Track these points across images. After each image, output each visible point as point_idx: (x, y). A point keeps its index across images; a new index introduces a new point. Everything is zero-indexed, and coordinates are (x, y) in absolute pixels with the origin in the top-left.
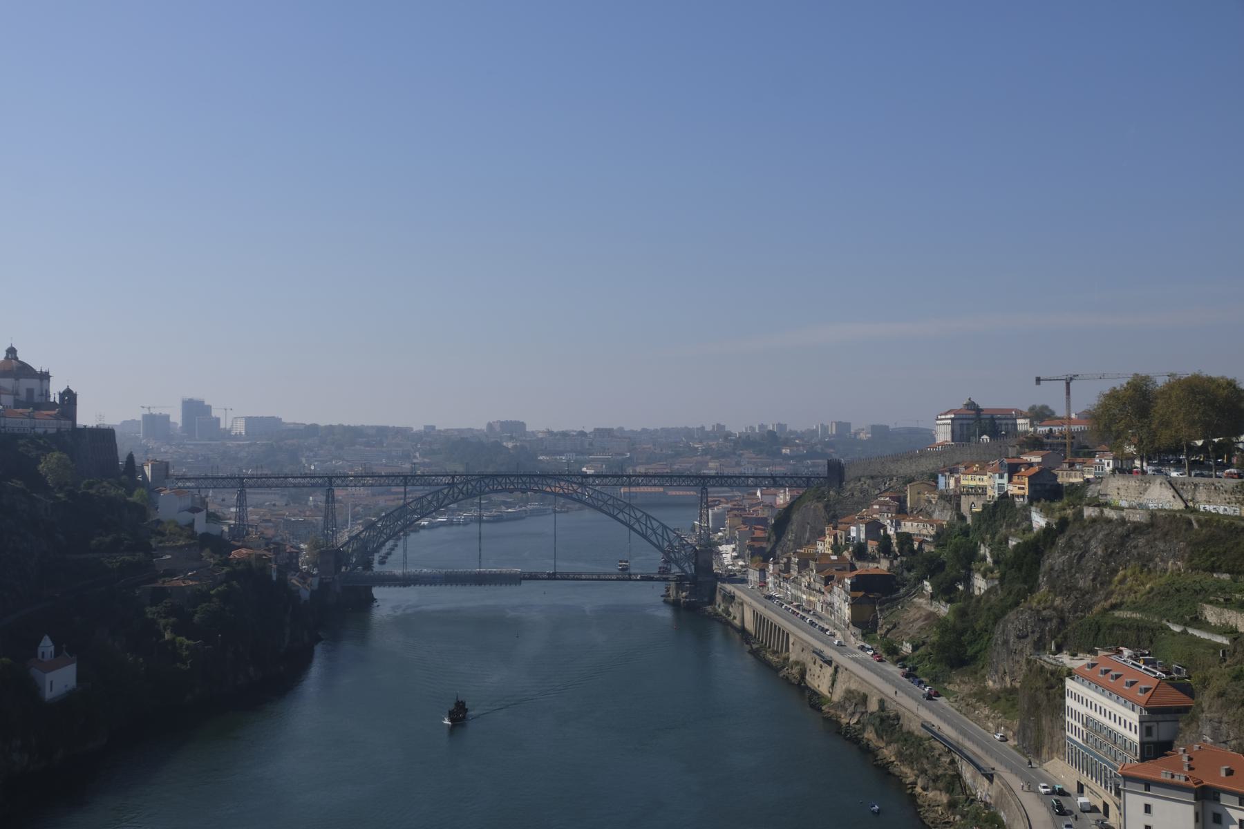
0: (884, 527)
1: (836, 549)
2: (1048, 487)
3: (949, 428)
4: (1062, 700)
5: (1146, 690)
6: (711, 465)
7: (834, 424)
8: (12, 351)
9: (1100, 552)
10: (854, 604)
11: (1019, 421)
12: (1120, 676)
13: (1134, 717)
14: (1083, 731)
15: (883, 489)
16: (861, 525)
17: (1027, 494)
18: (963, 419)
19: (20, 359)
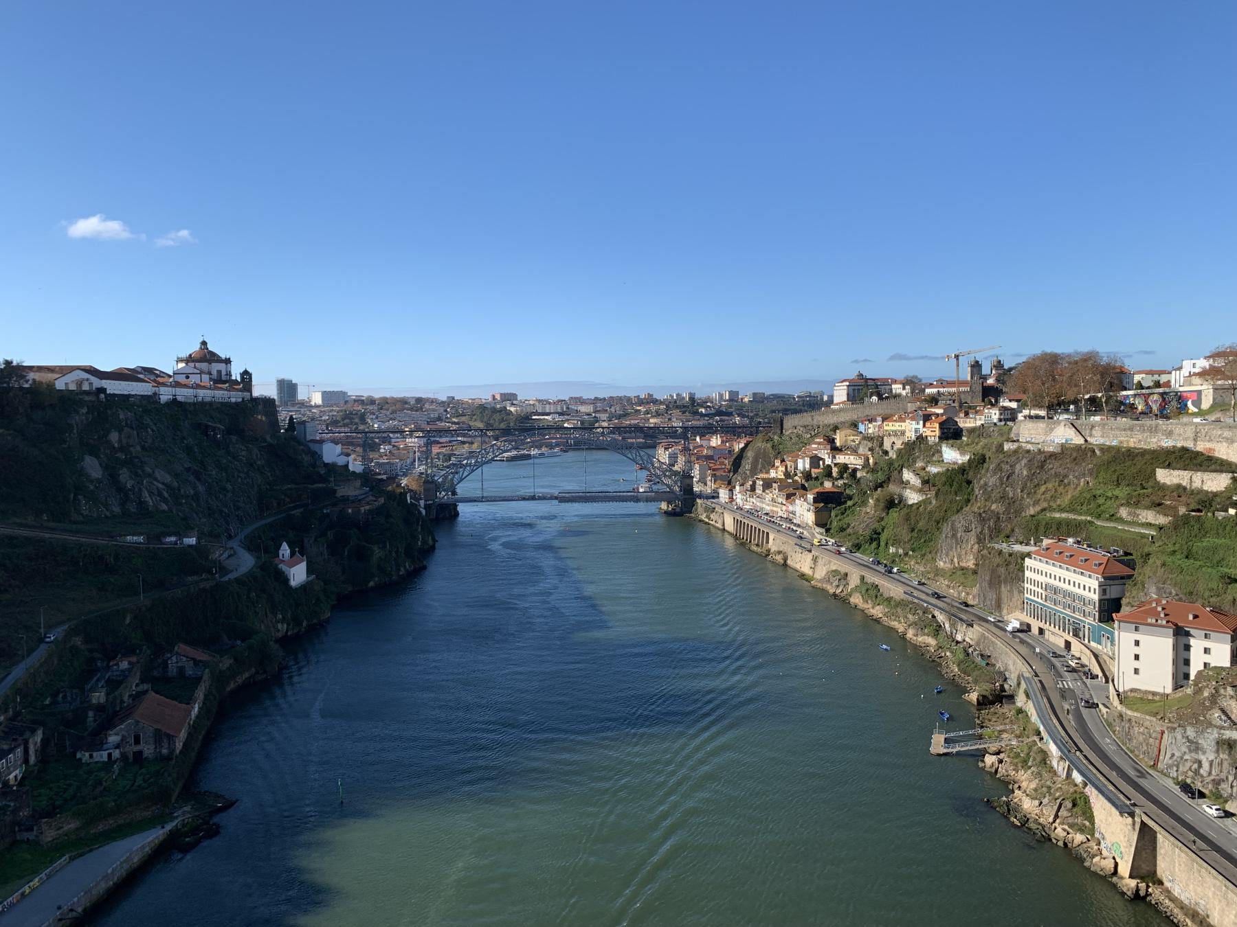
0: (823, 460)
1: (787, 475)
2: (952, 431)
3: (845, 392)
4: (1021, 574)
5: (1100, 564)
6: (651, 421)
7: (727, 392)
8: (204, 343)
9: (1025, 473)
10: (818, 512)
11: (894, 386)
12: (1073, 555)
13: (1094, 584)
14: (1042, 594)
15: (813, 434)
16: (806, 458)
17: (938, 435)
18: (854, 386)
19: (210, 349)
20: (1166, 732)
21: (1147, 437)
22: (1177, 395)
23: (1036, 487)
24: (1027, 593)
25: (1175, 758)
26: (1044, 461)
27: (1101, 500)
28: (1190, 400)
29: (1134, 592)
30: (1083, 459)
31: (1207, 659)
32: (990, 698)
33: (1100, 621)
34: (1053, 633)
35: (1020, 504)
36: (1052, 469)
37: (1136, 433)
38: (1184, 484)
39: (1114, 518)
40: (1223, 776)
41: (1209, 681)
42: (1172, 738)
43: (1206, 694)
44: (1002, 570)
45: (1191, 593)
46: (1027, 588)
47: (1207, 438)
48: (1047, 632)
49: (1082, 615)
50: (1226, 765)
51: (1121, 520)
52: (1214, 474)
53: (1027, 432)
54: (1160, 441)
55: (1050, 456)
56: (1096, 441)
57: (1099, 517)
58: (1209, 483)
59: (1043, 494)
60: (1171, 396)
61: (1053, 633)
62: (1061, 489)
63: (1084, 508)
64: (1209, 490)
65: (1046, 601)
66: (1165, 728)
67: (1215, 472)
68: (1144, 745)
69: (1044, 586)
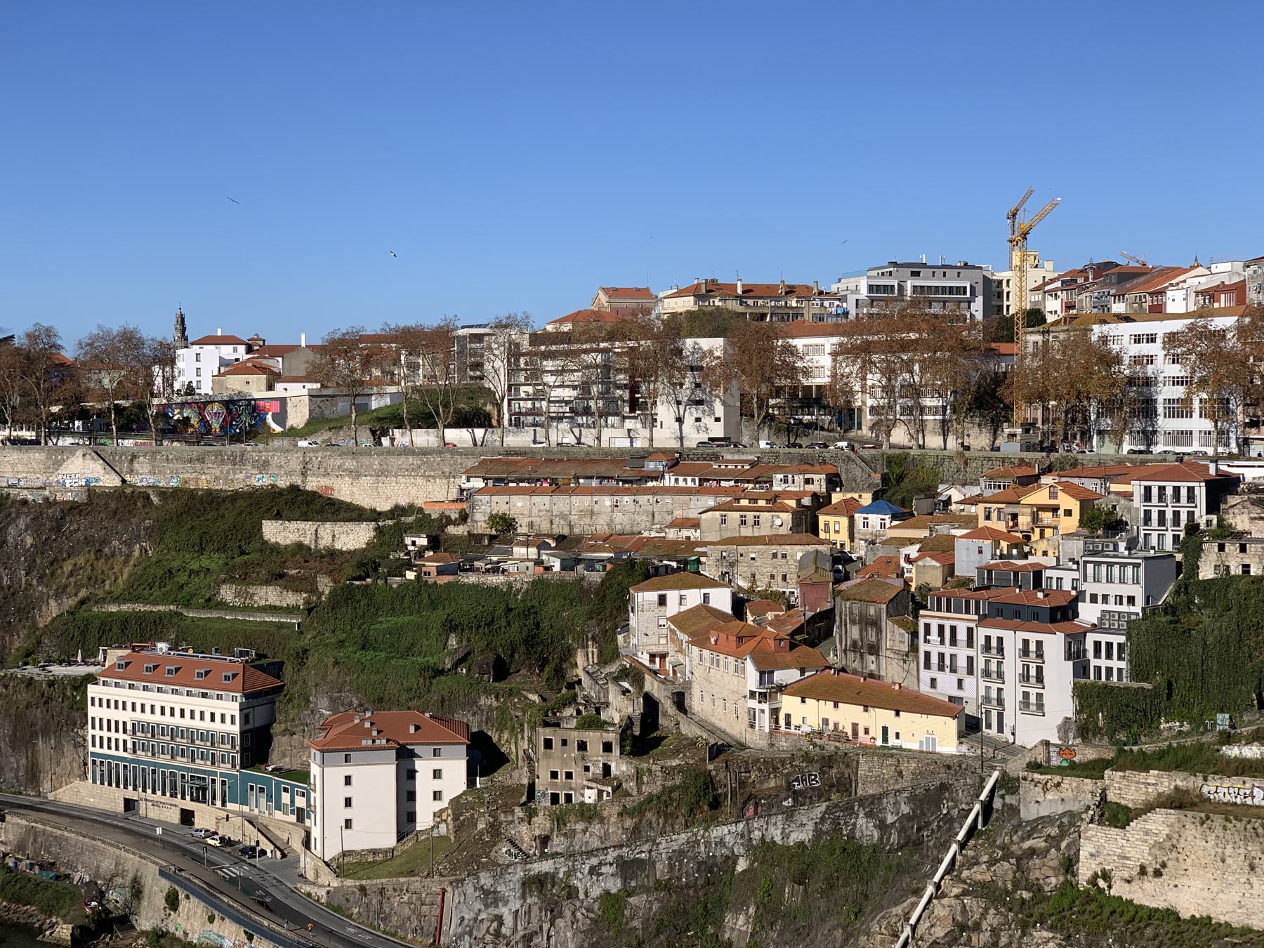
5: (234, 676)
13: (230, 706)
20: (449, 889)
21: (228, 472)
22: (249, 404)
23: (52, 563)
24: (94, 745)
25: (466, 922)
26: (61, 519)
27: (182, 578)
28: (270, 413)
29: (292, 713)
30: (130, 512)
31: (437, 785)
32: (92, 926)
33: (242, 767)
34: (155, 804)
35: (26, 597)
36: (76, 531)
37: (210, 465)
38: (307, 542)
39: (212, 603)
40: (534, 926)
41: (473, 809)
42: (459, 896)
43: (481, 826)
44: (38, 714)
45: (381, 700)
46: (93, 737)
47: (322, 470)
48: (142, 804)
49: (209, 763)
50: (535, 909)
51: (223, 605)
52: (350, 525)
53: (8, 469)
54: (250, 478)
55: (71, 509)
56: (141, 481)
57: (188, 605)
58: (343, 538)
59: (71, 574)
60: (240, 406)
61: (155, 804)
62: (100, 564)
63: (156, 592)
64: (344, 549)
65: (134, 752)
66: (445, 885)
67: (352, 520)
68: (414, 918)
69: (129, 727)
